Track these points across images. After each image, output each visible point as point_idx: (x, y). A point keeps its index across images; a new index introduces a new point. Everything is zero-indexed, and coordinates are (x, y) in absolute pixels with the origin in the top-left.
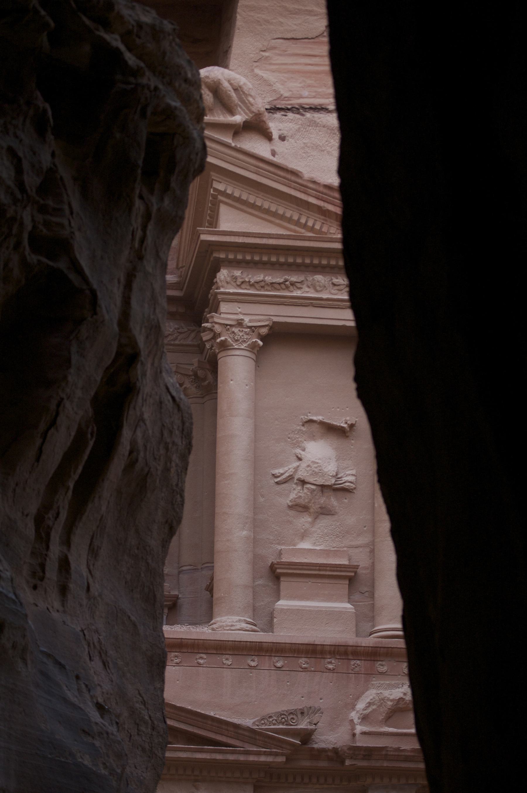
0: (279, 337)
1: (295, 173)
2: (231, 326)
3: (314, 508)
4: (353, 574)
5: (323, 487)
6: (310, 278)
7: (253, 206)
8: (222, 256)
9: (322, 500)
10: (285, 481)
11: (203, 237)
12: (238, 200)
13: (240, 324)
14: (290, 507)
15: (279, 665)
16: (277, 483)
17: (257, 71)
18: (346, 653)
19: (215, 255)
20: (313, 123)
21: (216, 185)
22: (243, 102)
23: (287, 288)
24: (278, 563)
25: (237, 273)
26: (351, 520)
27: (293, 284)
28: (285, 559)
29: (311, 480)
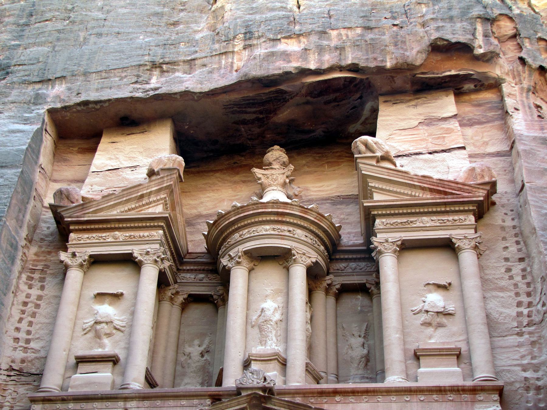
0: (406, 247)
1: (405, 173)
2: (383, 242)
3: (434, 323)
4: (458, 353)
5: (438, 312)
6: (420, 219)
7: (389, 191)
8: (376, 213)
9: (438, 320)
10: (418, 313)
11: (365, 204)
12: (382, 189)
13: (387, 241)
14: (422, 324)
15: (422, 399)
16: (414, 314)
17: (388, 143)
18: (458, 390)
19: (373, 213)
20: (417, 159)
21: (370, 184)
22: (379, 148)
23: (409, 224)
24: (417, 350)
25: (384, 220)
26: (455, 329)
27: (411, 222)
28: (421, 347)
29: (431, 310)
